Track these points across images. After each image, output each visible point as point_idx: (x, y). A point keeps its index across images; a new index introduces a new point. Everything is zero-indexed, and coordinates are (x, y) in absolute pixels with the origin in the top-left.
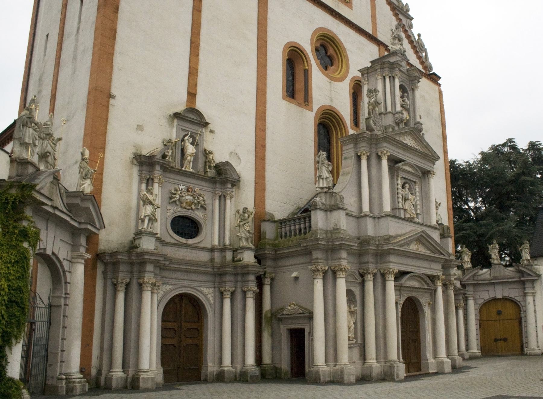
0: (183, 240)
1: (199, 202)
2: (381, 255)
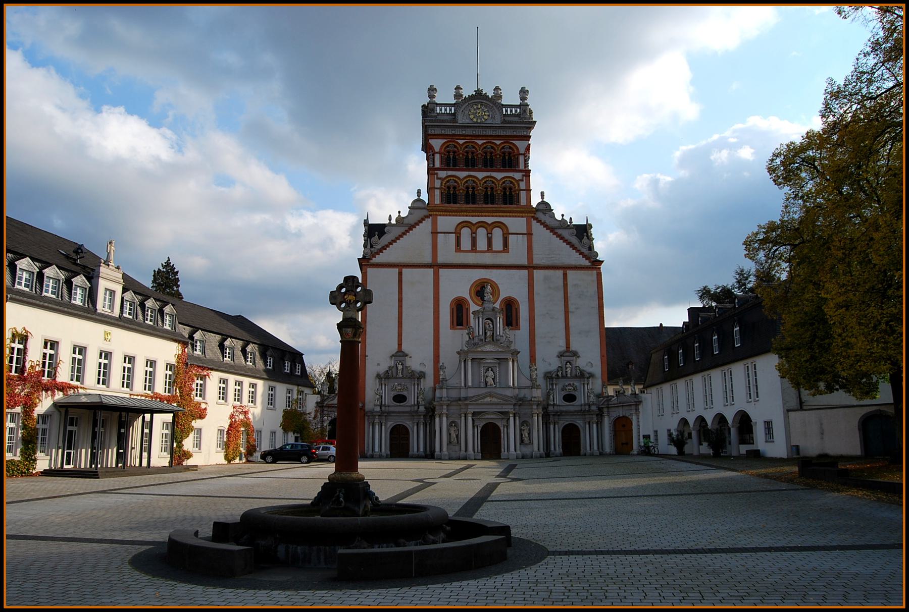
2: (467, 405)
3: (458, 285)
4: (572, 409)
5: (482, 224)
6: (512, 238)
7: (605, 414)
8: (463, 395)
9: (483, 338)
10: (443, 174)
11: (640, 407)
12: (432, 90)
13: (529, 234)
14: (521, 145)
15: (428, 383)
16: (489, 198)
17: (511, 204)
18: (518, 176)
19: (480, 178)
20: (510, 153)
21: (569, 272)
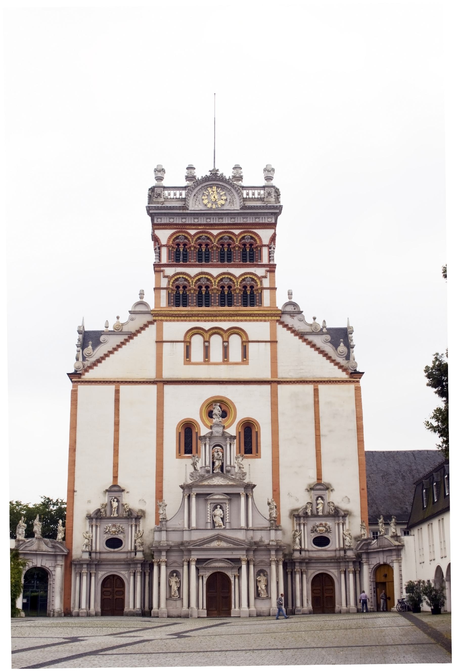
0: (112, 550)
1: (119, 530)
2: (190, 551)
3: (186, 404)
4: (324, 555)
5: (216, 331)
6: (251, 347)
7: (364, 560)
8: (186, 537)
9: (210, 469)
10: (170, 271)
11: (403, 553)
12: (160, 172)
13: (273, 342)
14: (264, 235)
15: (149, 523)
16: (226, 299)
17: (252, 305)
18: (260, 272)
19: (215, 275)
20: (251, 245)
21: (321, 387)
